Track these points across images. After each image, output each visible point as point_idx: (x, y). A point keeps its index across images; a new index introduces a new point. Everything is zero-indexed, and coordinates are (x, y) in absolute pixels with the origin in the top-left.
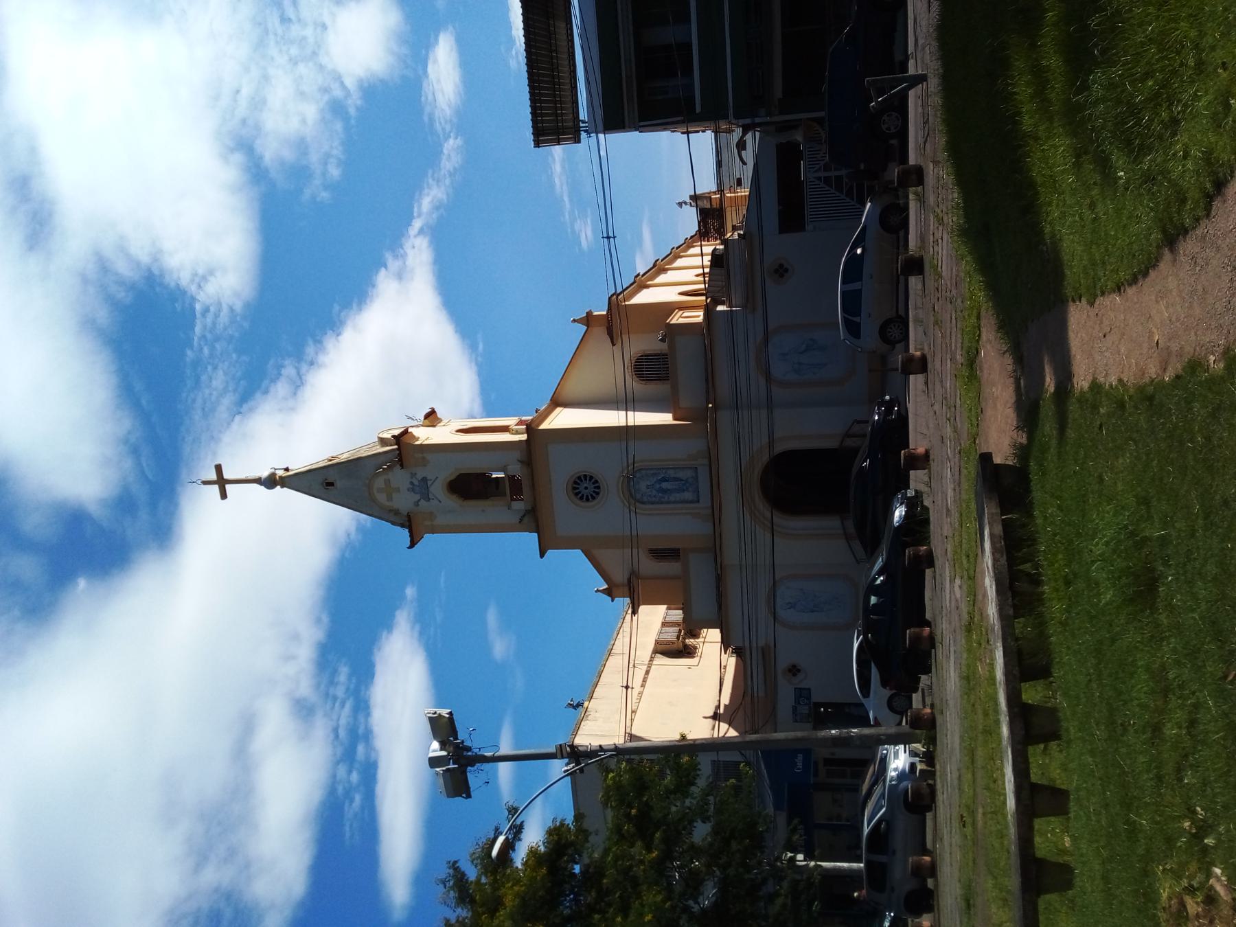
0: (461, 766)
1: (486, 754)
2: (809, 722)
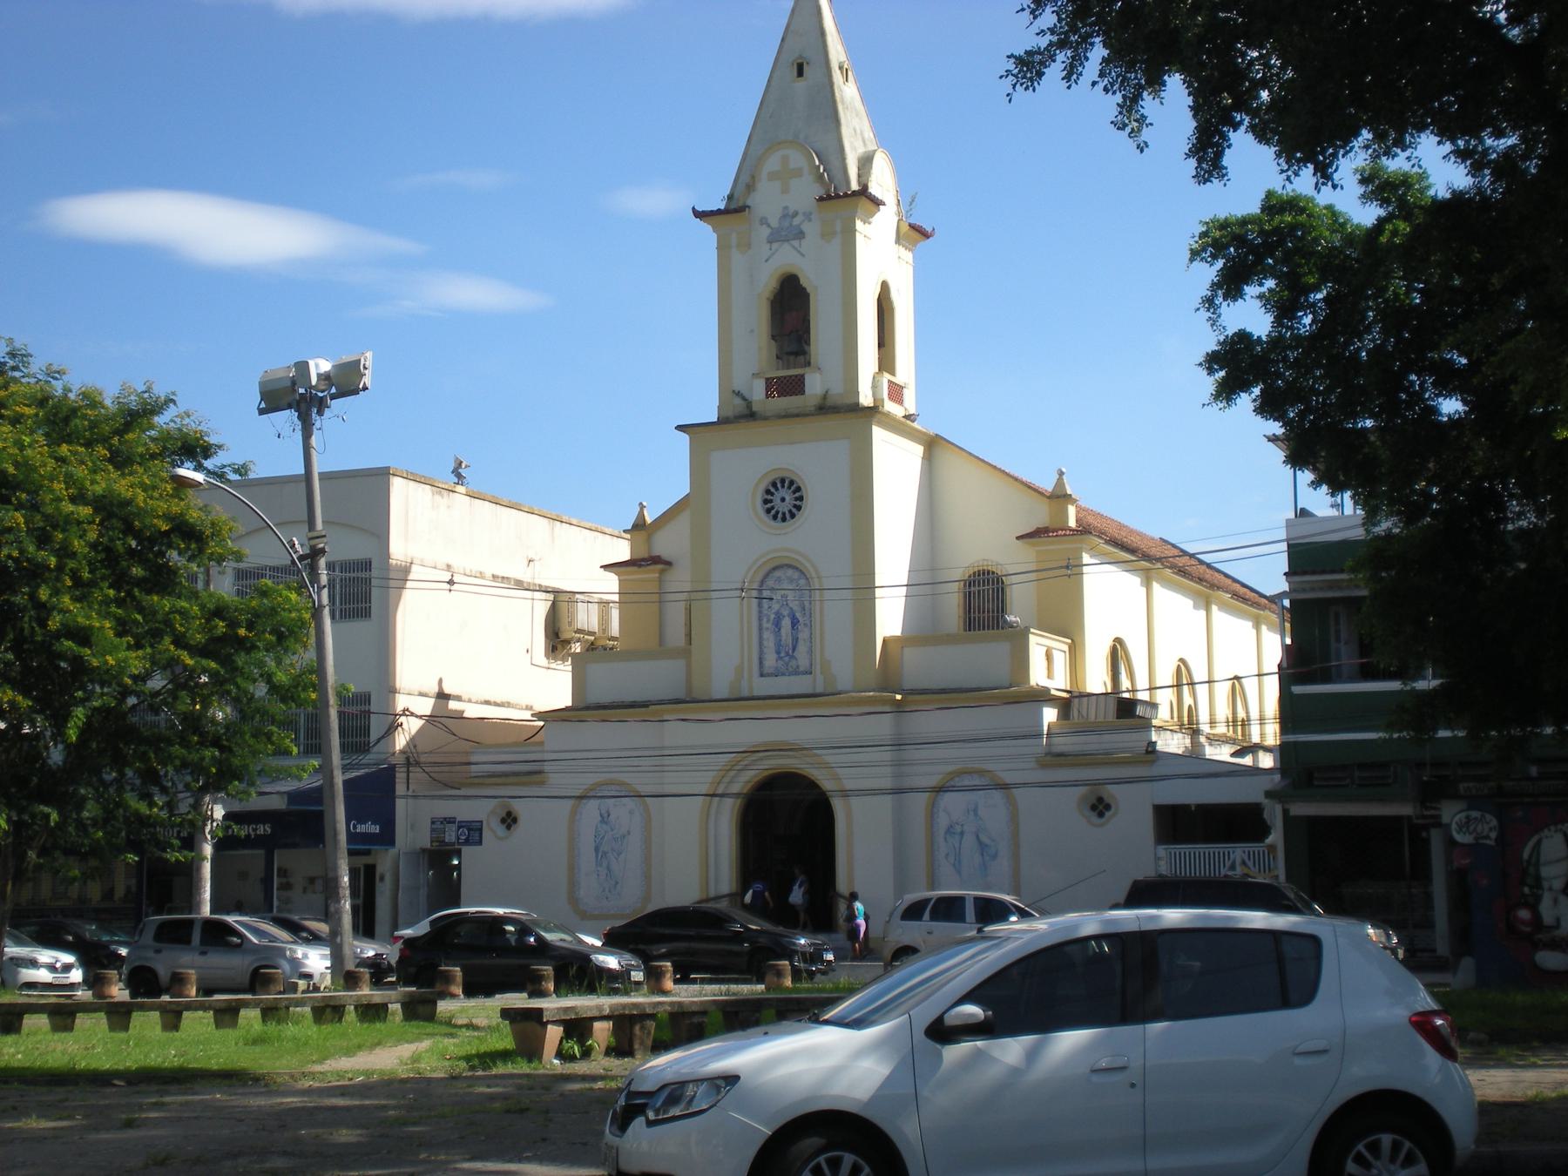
1: (313, 437)
2: (432, 842)
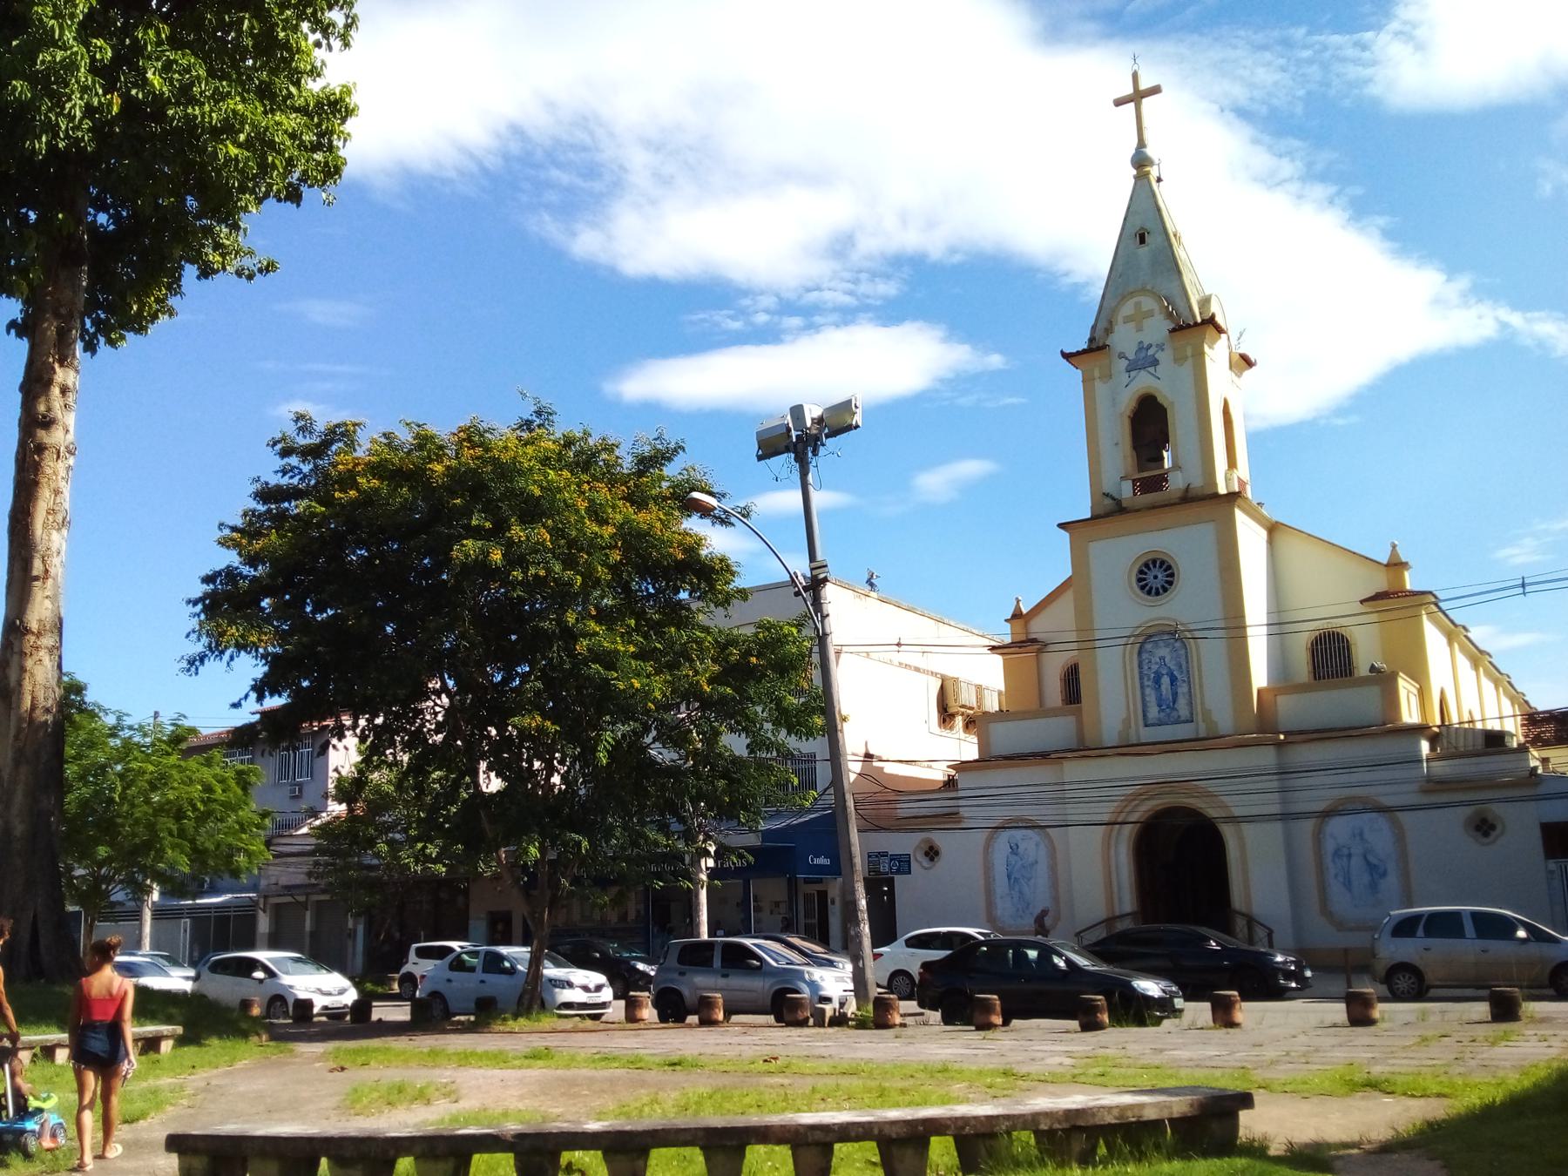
0: (795, 445)
1: (810, 475)
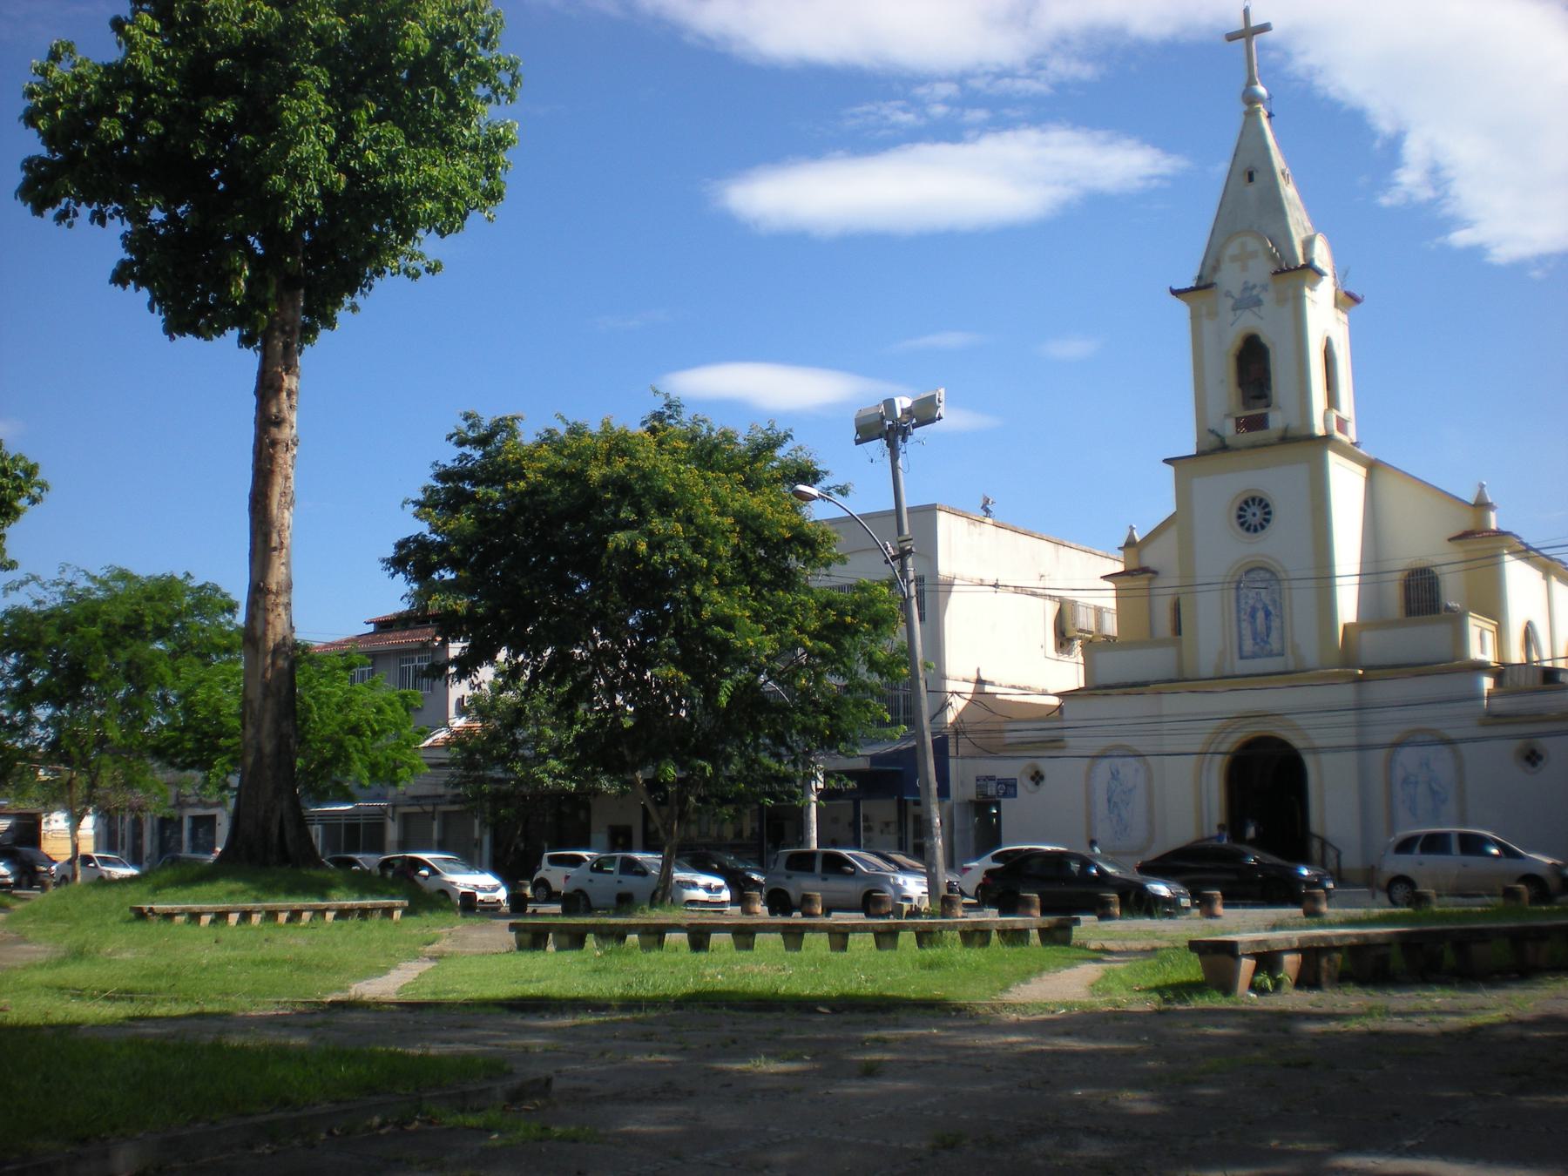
0: (887, 433)
1: (900, 460)
